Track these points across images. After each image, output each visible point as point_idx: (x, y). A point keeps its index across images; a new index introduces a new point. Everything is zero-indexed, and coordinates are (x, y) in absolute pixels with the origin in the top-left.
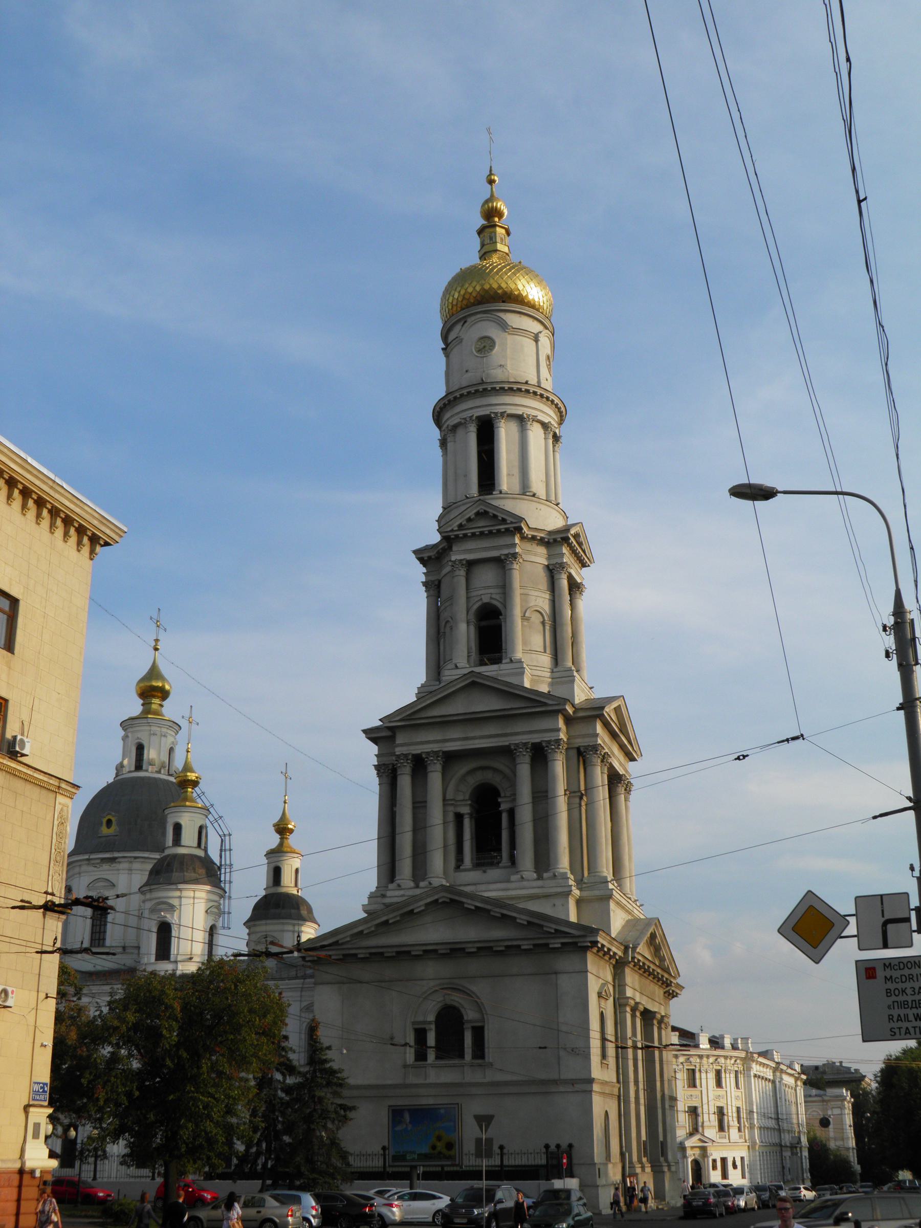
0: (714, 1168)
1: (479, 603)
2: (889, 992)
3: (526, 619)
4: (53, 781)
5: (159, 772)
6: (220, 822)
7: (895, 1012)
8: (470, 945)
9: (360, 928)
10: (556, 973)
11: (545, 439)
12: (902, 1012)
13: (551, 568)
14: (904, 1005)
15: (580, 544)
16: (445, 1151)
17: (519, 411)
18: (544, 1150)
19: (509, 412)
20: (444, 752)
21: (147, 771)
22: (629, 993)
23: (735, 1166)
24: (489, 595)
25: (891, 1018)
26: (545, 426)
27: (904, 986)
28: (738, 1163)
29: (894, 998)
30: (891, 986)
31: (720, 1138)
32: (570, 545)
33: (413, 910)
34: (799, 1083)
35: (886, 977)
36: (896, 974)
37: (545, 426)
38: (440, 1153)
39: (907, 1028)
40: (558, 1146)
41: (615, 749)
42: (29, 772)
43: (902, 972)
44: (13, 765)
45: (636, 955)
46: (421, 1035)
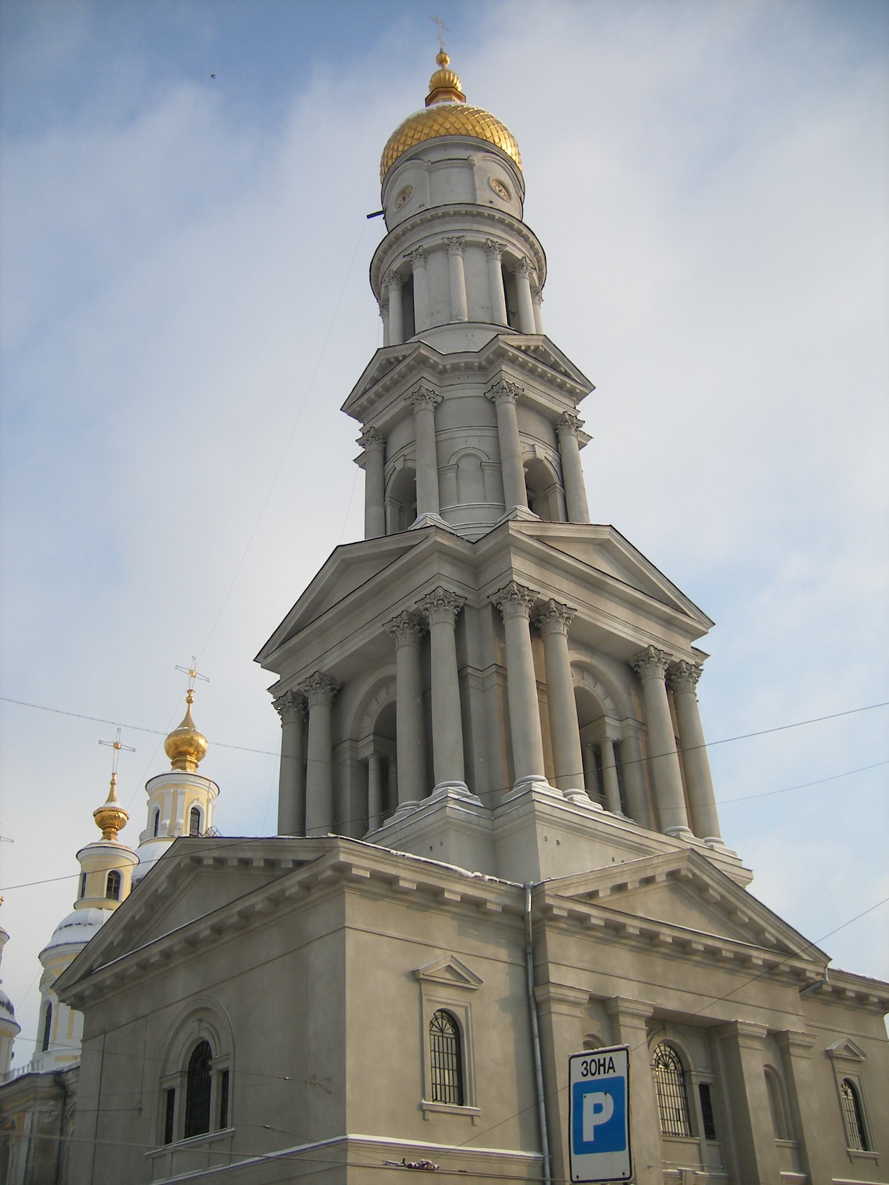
1: (395, 473)
3: (450, 469)
8: (202, 926)
9: (109, 940)
10: (308, 944)
11: (487, 262)
13: (488, 395)
15: (554, 366)
17: (437, 241)
19: (425, 247)
20: (323, 676)
22: (555, 975)
24: (403, 457)
26: (487, 248)
32: (513, 360)
33: (156, 891)
37: (487, 248)
41: (622, 612)
45: (549, 901)
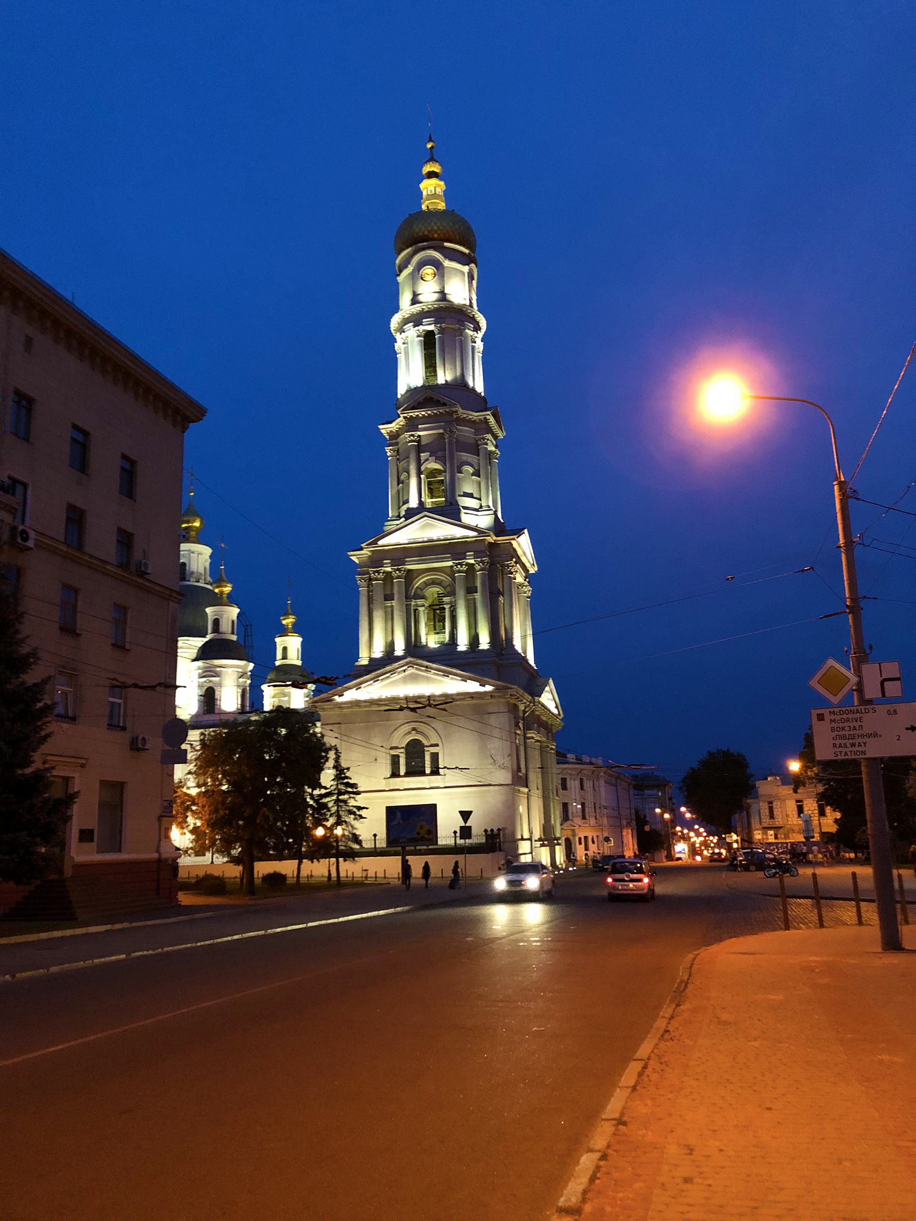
0: (580, 843)
2: (833, 730)
4: (168, 592)
5: (198, 582)
6: (243, 616)
7: (838, 742)
12: (843, 742)
14: (843, 737)
16: (426, 836)
18: (484, 833)
21: (189, 581)
23: (593, 842)
25: (835, 745)
27: (843, 725)
28: (595, 840)
29: (836, 733)
30: (835, 725)
31: (584, 823)
34: (631, 787)
35: (831, 720)
36: (838, 718)
38: (423, 837)
39: (846, 752)
40: (492, 830)
42: (151, 585)
43: (842, 717)
44: (140, 580)
46: (395, 760)
